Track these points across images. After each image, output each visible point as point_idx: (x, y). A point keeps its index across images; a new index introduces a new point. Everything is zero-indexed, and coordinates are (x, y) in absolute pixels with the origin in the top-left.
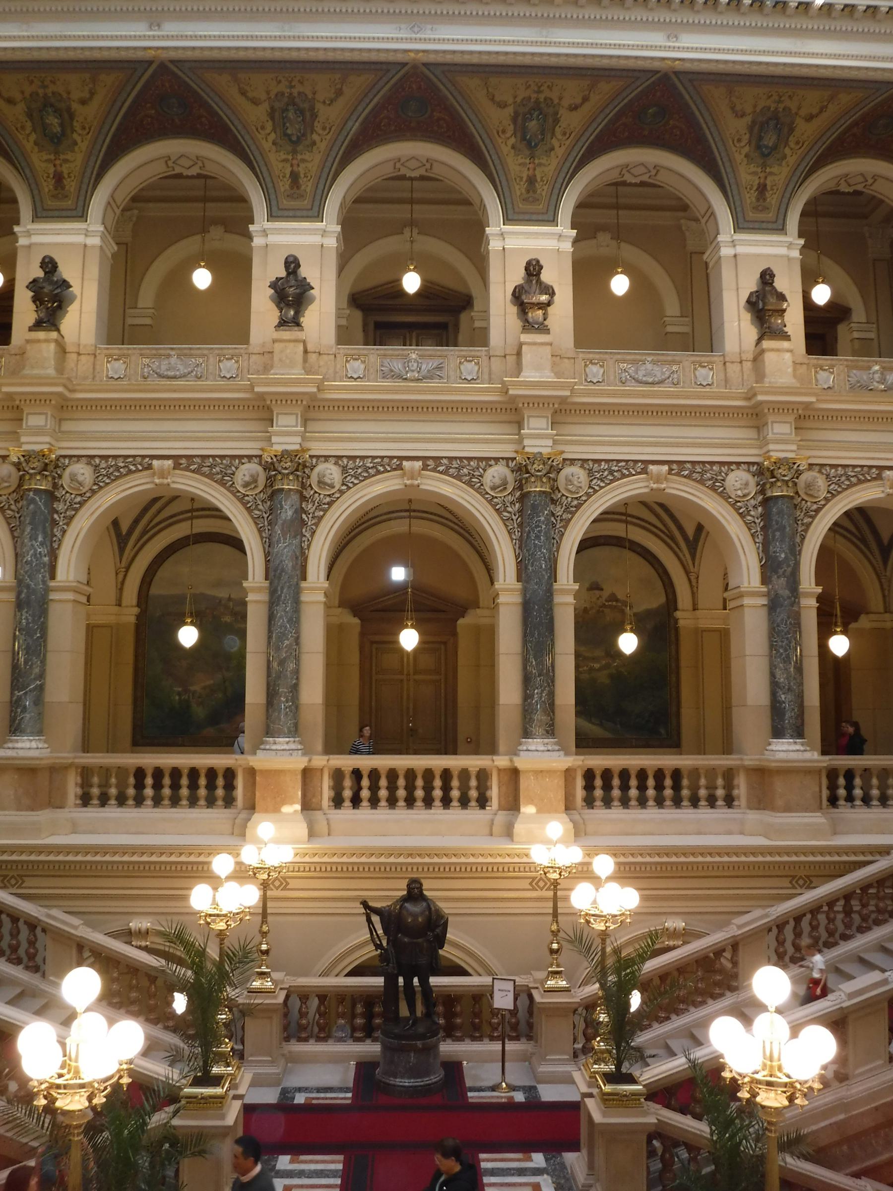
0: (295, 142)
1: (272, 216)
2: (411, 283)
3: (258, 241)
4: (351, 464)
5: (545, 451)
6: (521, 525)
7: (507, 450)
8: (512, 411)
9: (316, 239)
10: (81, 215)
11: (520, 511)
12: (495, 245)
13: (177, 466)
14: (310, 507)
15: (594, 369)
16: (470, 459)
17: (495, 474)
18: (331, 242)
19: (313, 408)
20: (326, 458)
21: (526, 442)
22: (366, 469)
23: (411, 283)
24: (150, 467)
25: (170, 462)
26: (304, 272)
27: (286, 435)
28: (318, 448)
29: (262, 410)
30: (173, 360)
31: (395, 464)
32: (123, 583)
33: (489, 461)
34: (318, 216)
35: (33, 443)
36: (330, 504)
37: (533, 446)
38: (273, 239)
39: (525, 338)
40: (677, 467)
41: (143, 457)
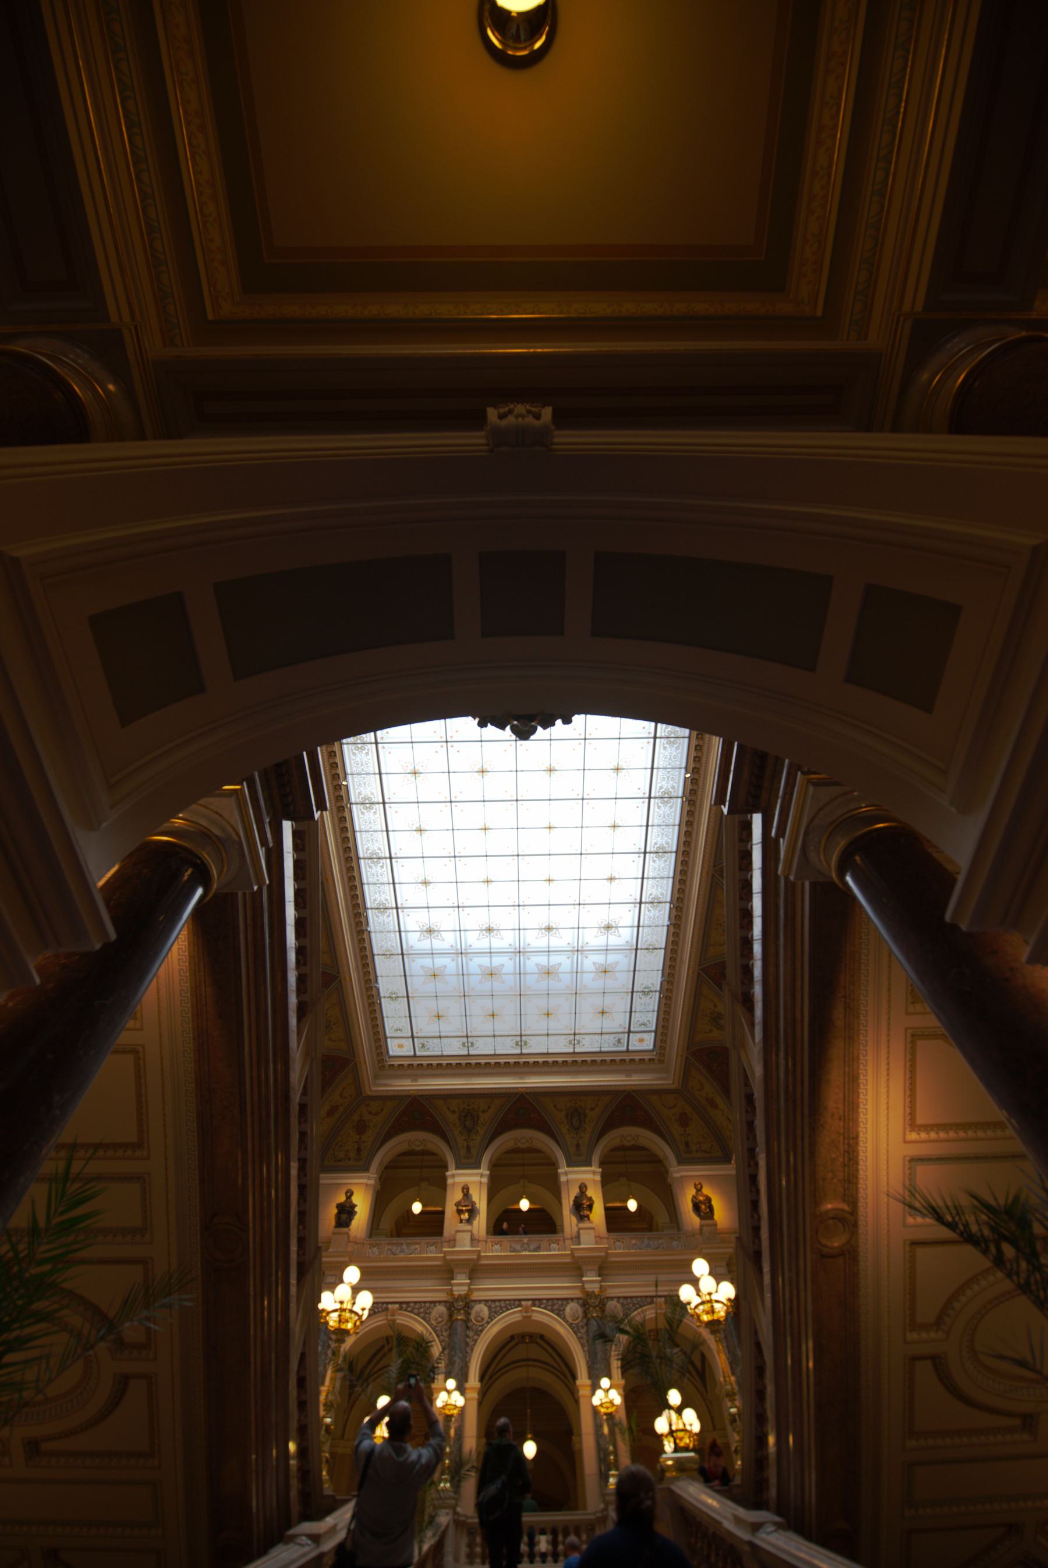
0: (470, 1131)
1: (457, 1168)
4: (493, 1305)
5: (597, 1291)
6: (588, 1341)
8: (575, 1268)
10: (366, 1169)
11: (587, 1331)
12: (563, 1179)
13: (401, 1308)
14: (471, 1334)
16: (558, 1299)
17: (571, 1309)
18: (485, 1180)
19: (476, 1269)
20: (480, 1301)
21: (587, 1286)
22: (501, 1308)
24: (387, 1309)
25: (397, 1306)
26: (471, 1192)
27: (460, 1284)
29: (447, 1271)
30: (404, 1246)
31: (518, 1302)
32: (347, 1421)
33: (567, 1300)
34: (479, 1167)
36: (481, 1331)
37: (589, 1287)
39: (581, 1225)
41: (383, 1303)
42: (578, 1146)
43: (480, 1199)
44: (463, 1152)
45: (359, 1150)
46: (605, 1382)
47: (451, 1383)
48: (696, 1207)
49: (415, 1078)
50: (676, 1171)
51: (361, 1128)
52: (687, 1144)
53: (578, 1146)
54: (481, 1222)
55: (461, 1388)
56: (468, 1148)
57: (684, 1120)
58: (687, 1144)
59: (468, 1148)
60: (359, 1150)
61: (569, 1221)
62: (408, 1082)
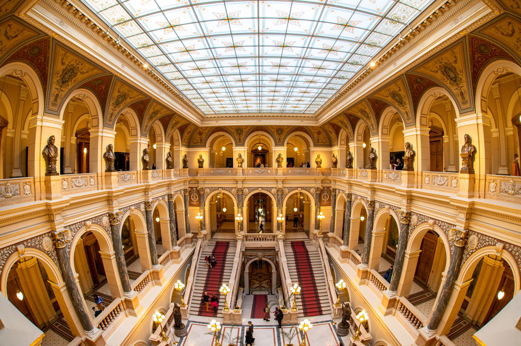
2: (260, 148)
3: (234, 150)
7: (275, 186)
9: (244, 150)
15: (290, 171)
18: (246, 150)
23: (260, 148)
27: (240, 186)
28: (244, 186)
35: (200, 186)
38: (236, 150)
40: (302, 188)
42: (280, 139)
43: (245, 157)
44: (238, 140)
45: (201, 140)
46: (281, 215)
47: (239, 215)
48: (317, 162)
49: (217, 121)
50: (312, 149)
51: (200, 134)
52: (318, 140)
53: (280, 139)
54: (245, 165)
55: (242, 216)
56: (240, 139)
57: (319, 133)
58: (318, 140)
59: (240, 139)
60: (201, 140)
61: (275, 164)
62: (214, 122)
